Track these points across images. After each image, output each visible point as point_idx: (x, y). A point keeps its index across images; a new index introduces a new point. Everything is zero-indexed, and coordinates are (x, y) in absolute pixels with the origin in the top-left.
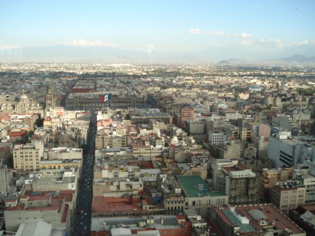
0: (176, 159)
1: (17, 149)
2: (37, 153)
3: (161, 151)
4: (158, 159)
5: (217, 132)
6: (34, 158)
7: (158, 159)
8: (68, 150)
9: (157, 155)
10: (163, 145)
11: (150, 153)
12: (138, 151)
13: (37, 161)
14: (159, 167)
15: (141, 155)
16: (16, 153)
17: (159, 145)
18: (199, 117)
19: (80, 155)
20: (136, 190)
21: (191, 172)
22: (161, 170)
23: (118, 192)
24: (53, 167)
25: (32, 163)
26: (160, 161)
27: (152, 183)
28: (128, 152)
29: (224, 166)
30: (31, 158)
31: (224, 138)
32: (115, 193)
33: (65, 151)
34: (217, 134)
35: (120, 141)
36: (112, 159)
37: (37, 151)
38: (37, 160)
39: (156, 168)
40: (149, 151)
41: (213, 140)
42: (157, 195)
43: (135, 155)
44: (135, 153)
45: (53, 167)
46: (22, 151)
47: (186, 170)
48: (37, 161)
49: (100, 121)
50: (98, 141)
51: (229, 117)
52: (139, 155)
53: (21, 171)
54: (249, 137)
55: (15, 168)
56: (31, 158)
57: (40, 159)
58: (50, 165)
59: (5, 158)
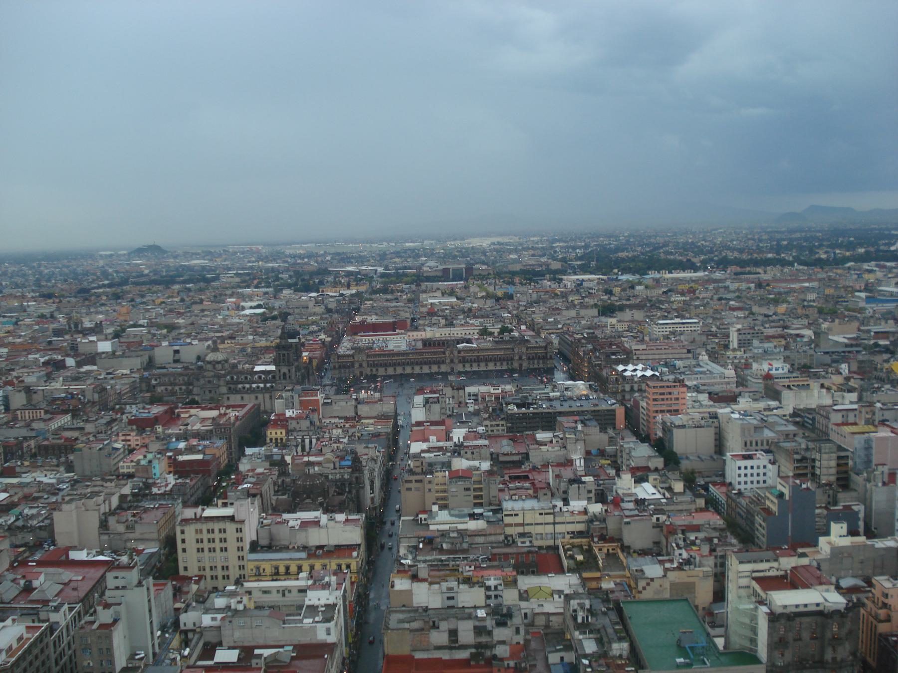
0: (626, 543)
1: (186, 521)
3: (584, 518)
4: (577, 541)
5: (749, 457)
6: (232, 545)
7: (577, 541)
8: (324, 519)
10: (589, 499)
11: (554, 523)
12: (519, 520)
13: (241, 554)
14: (578, 568)
15: (528, 529)
16: (183, 532)
17: (579, 499)
18: (701, 406)
19: (354, 535)
20: (503, 642)
21: (667, 585)
22: (581, 576)
23: (455, 648)
24: (282, 570)
25: (226, 559)
26: (580, 547)
27: (552, 618)
28: (488, 522)
29: (755, 575)
30: (223, 545)
31: (770, 474)
32: (447, 651)
33: (316, 523)
34: (749, 463)
35: (468, 489)
36: (445, 546)
37: (239, 526)
38: (240, 549)
39: (570, 570)
40: (550, 518)
41: (738, 479)
42: (562, 659)
43: (509, 531)
44: (510, 525)
45: (282, 570)
46: (199, 526)
47: (652, 580)
48: (241, 554)
49: (419, 424)
50: (409, 489)
51: (791, 401)
52: (520, 530)
53: (197, 582)
54: (844, 469)
55: (182, 572)
56: (223, 545)
58: (274, 563)
59: (159, 540)
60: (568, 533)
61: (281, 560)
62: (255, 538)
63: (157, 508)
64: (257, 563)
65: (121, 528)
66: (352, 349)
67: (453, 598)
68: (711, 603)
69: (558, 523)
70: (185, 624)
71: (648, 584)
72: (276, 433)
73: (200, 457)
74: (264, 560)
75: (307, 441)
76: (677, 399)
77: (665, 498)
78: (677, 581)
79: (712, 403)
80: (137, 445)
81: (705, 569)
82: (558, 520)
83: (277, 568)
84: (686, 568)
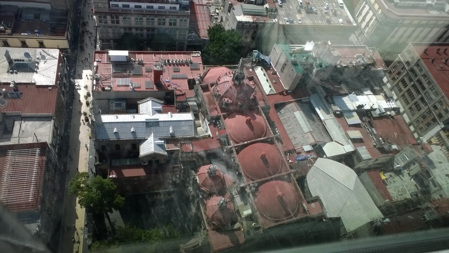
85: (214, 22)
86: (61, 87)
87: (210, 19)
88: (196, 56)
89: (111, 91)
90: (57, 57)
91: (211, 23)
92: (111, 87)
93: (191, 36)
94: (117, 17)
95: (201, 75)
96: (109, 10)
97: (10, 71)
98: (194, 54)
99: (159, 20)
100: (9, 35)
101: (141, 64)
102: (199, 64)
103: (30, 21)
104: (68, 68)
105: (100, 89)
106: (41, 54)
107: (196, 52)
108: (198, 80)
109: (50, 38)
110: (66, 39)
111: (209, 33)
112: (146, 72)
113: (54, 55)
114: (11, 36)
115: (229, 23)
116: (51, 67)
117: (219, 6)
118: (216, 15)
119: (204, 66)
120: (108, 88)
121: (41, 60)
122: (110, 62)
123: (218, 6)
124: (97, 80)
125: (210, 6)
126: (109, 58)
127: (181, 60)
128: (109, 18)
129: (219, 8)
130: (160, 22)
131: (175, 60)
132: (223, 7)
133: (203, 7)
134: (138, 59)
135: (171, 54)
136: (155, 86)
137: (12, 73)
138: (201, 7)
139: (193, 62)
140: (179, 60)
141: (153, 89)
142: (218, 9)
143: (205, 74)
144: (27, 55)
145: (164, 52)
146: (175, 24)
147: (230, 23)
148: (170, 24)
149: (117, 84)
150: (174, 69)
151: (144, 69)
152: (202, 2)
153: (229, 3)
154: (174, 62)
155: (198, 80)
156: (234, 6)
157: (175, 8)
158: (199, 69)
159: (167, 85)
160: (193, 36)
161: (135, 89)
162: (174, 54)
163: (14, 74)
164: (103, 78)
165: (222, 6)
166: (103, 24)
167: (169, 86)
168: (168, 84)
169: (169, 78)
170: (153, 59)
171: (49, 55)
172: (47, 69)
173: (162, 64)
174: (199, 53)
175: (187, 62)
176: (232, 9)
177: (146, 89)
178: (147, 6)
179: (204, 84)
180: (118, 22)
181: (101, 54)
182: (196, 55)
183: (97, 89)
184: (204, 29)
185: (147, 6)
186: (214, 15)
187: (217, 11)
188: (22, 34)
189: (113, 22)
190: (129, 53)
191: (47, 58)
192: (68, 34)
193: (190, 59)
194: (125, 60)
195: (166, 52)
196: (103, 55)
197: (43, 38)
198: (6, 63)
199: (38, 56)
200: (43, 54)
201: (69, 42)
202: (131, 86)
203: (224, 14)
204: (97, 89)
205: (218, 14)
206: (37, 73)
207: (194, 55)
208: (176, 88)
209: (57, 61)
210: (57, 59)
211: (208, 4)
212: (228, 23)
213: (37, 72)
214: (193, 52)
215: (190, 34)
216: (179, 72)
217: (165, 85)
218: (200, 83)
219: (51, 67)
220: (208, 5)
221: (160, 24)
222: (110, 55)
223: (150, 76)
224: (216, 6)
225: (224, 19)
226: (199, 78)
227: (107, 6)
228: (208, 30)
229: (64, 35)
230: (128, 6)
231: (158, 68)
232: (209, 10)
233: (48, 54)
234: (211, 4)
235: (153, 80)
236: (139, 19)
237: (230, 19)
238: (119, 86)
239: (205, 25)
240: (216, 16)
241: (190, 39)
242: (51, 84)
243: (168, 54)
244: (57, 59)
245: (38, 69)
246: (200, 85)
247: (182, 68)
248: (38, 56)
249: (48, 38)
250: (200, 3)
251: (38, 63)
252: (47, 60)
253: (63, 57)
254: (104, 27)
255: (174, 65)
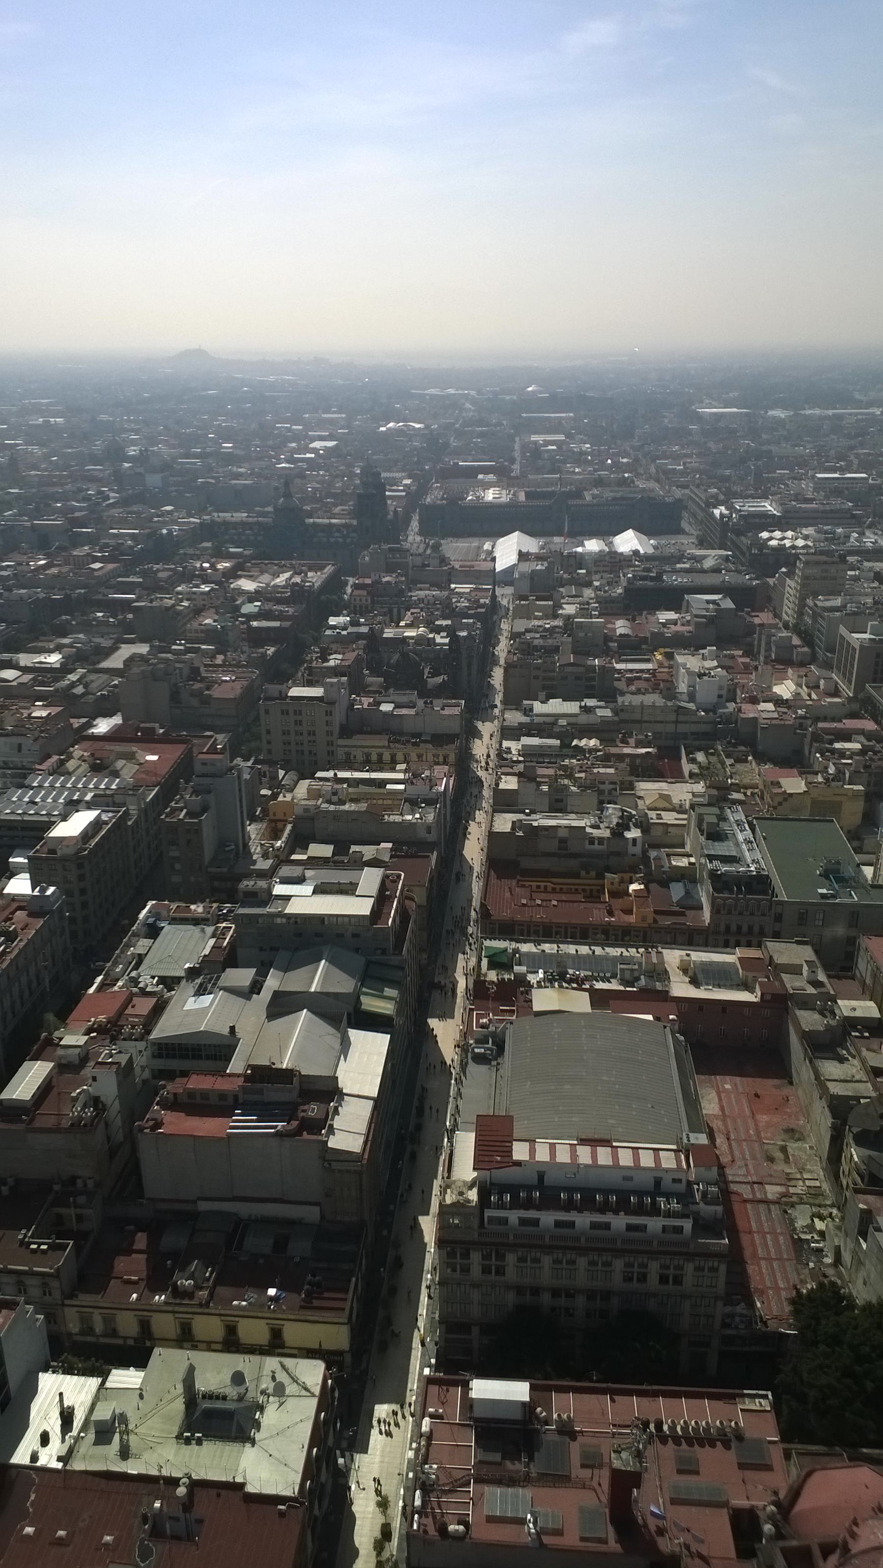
2: (329, 713)
9: (694, 728)
11: (677, 722)
16: (267, 712)
24: (374, 757)
38: (329, 733)
45: (374, 757)
47: (791, 795)
57: (336, 731)
58: (366, 750)
60: (692, 734)
61: (373, 747)
62: (344, 722)
63: (234, 681)
64: (347, 749)
65: (195, 702)
66: (443, 499)
67: (562, 801)
68: (859, 826)
69: (681, 722)
70: (274, 815)
71: (785, 800)
72: (361, 600)
73: (276, 624)
74: (354, 746)
75: (395, 611)
76: (834, 578)
77: (811, 700)
78: (821, 798)
79: (876, 584)
80: (204, 605)
81: (855, 787)
82: (681, 718)
83: (368, 755)
84: (833, 784)
85: (811, 1265)
86: (311, 1503)
87: (795, 1251)
88: (754, 1408)
89: (467, 1540)
90: (317, 1390)
91: (799, 1267)
92: (466, 1524)
93: (732, 1316)
94: (501, 1257)
95: (782, 1494)
96: (480, 1235)
97: (185, 1434)
98: (747, 1400)
99: (627, 1265)
100: (201, 1305)
101: (567, 1431)
102: (770, 1442)
103: (261, 1261)
104: (338, 1425)
105: (432, 1531)
106: (274, 1378)
107: (754, 1392)
108: (771, 1518)
109: (302, 1318)
110: (346, 1321)
111: (796, 1313)
112: (583, 1466)
113: (309, 1383)
114: (206, 1311)
115: (865, 1274)
116: (297, 1423)
117: (825, 1206)
118: (816, 1237)
119: (786, 1446)
120: (457, 1527)
121: (271, 1398)
122: (470, 1418)
123: (820, 1206)
124: (427, 1488)
125: (793, 1205)
126: (469, 1404)
127: (704, 1423)
128: (476, 1257)
129: (824, 1212)
130: (628, 1272)
131: (682, 1422)
132: (839, 1209)
133: (769, 1210)
134: (559, 1415)
135: (666, 1395)
136: (611, 1529)
137: (188, 1441)
138: (762, 1207)
139: (748, 1435)
140: (696, 1423)
141: (604, 1541)
142: (822, 1218)
143: (796, 1494)
144: (238, 1378)
145: (644, 1387)
146: (678, 1281)
147: (872, 1276)
148: (663, 1279)
149: (486, 1511)
150: (680, 1460)
151: (575, 1449)
152: (765, 1193)
153: (861, 1206)
154: (679, 1428)
155: (771, 1518)
156: (879, 1219)
157: (679, 1230)
158: (769, 1468)
159: (653, 1528)
160: (741, 1315)
161: (546, 1539)
162: (677, 1395)
163: (194, 1447)
164: (444, 1485)
165: (832, 1206)
166: (457, 1275)
167: (661, 1532)
168: (660, 1523)
169: (661, 1501)
170: (604, 1413)
171: (295, 1380)
172: (283, 1431)
173: (641, 1446)
174: (765, 1397)
175: (726, 1435)
176: (871, 1229)
177: (583, 1539)
178: (591, 1222)
179: (794, 1543)
180: (500, 1271)
181: (445, 1388)
182: (755, 1405)
183: (422, 1527)
184: (777, 1289)
185: (591, 1222)
186: (809, 1237)
187: (819, 1225)
188: (235, 1303)
189: (486, 1270)
190: (532, 1388)
191: (288, 1391)
192: (349, 1301)
193: (736, 1423)
194: (518, 1415)
195: (649, 1388)
196: (451, 1389)
197: (285, 1316)
198: (179, 1406)
199: (267, 1384)
200: (281, 1377)
201: (352, 1330)
202: (531, 1525)
203: (845, 1240)
204: (422, 1527)
205: (822, 1234)
206: (253, 1446)
207: (749, 1405)
208: (688, 1547)
209: (314, 1402)
210: (313, 1395)
211: (784, 1199)
212: (862, 1274)
213: (253, 1442)
214: (746, 1392)
215: (729, 1309)
216: (697, 1473)
217: (646, 1525)
218: (779, 1535)
219: (297, 1423)
220: (786, 1203)
221: (631, 1279)
222: (473, 1397)
223: (595, 1483)
224: (815, 1205)
225: (847, 1257)
226: (773, 1508)
227: (475, 1223)
228: (792, 1302)
229: (344, 1309)
230: (536, 1222)
231: (623, 1461)
232: (792, 1221)
233: (293, 1378)
234: (794, 1199)
235: (605, 1499)
236: (564, 1261)
237: (867, 1262)
238: (491, 1519)
239: (778, 1275)
240: (817, 1242)
241: (729, 1332)
242: (288, 1493)
243: (655, 1394)
244: (313, 1395)
245: (259, 1431)
246: (781, 1543)
247: (704, 1454)
248: (267, 1384)
249: (298, 1317)
250: (759, 1196)
251: (261, 1408)
252: (289, 1399)
253: (333, 1389)
254: (459, 1284)
255: (677, 1440)
